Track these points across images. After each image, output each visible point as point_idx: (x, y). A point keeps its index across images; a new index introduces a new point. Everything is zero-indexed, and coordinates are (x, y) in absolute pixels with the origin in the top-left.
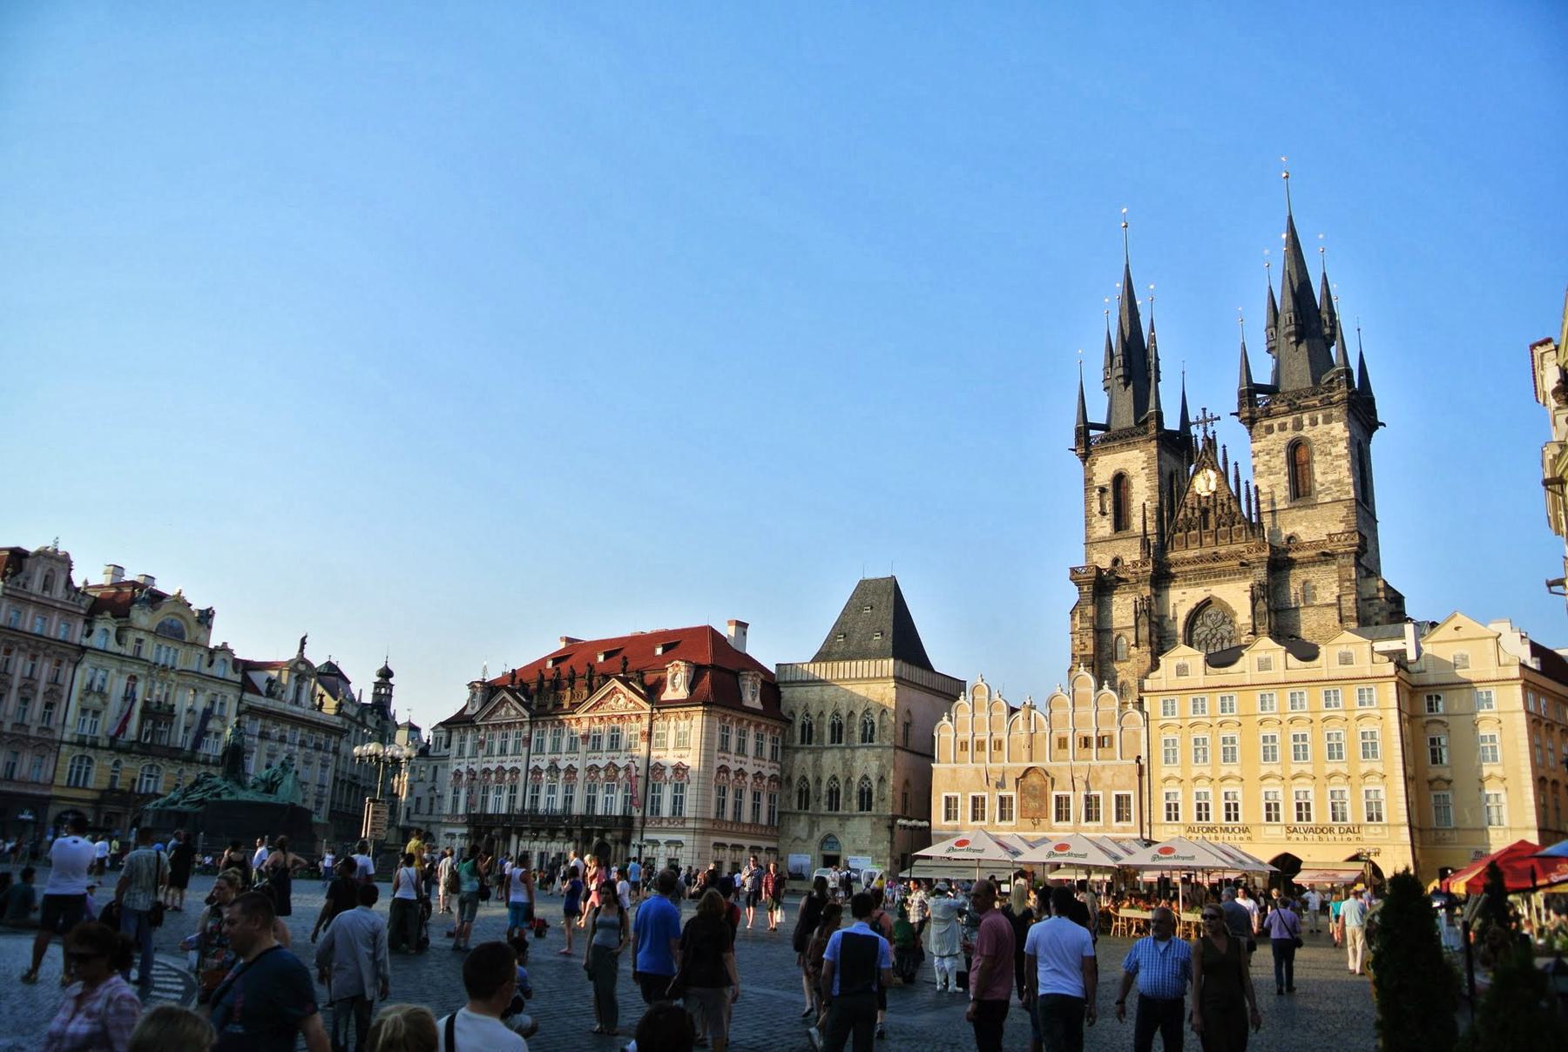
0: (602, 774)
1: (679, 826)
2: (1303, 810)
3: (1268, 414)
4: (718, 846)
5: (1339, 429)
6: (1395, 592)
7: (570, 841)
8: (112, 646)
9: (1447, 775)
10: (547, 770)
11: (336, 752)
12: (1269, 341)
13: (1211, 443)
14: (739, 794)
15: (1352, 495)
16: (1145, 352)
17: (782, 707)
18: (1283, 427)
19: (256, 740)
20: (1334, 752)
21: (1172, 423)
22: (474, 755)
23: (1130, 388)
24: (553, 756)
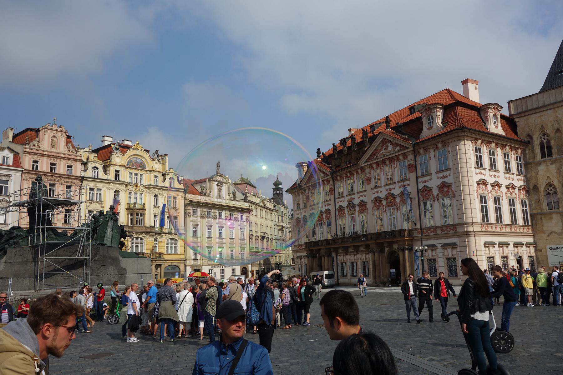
0: (384, 203)
1: (451, 231)
4: (487, 245)
7: (369, 252)
8: (102, 175)
10: (347, 207)
11: (248, 221)
14: (497, 201)
17: (519, 133)
19: (199, 219)
22: (305, 206)
24: (349, 197)
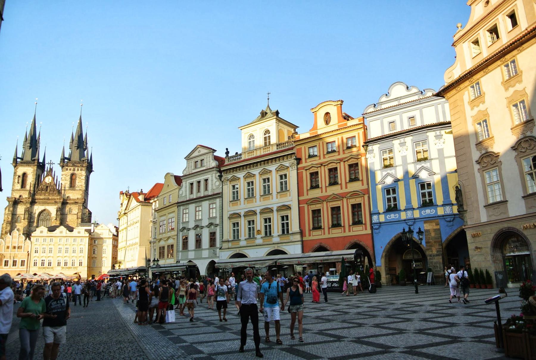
2: (66, 264)
3: (67, 166)
5: (84, 173)
6: (90, 212)
9: (96, 256)
12: (70, 146)
13: (51, 170)
15: (84, 189)
16: (36, 141)
18: (70, 170)
20: (74, 251)
21: (41, 160)
23: (31, 149)
